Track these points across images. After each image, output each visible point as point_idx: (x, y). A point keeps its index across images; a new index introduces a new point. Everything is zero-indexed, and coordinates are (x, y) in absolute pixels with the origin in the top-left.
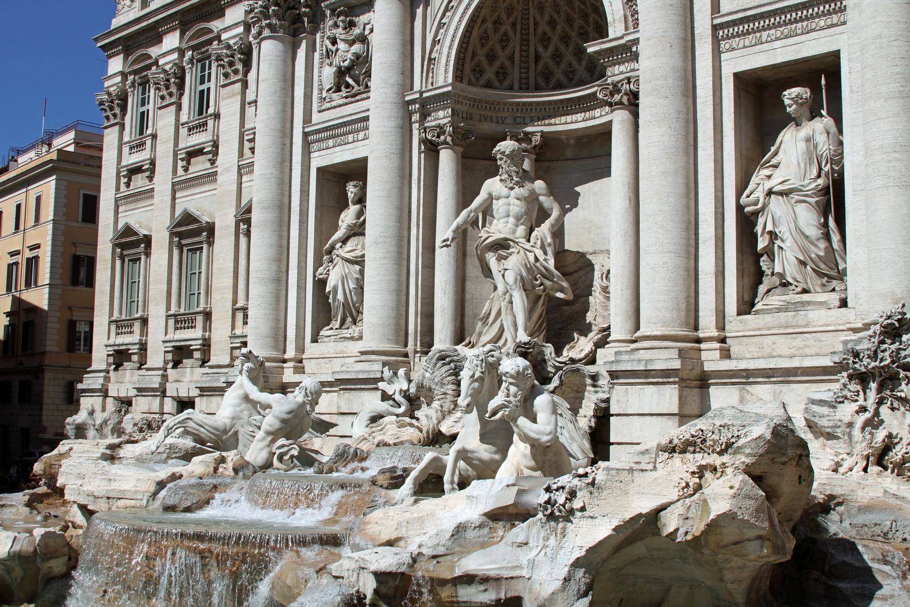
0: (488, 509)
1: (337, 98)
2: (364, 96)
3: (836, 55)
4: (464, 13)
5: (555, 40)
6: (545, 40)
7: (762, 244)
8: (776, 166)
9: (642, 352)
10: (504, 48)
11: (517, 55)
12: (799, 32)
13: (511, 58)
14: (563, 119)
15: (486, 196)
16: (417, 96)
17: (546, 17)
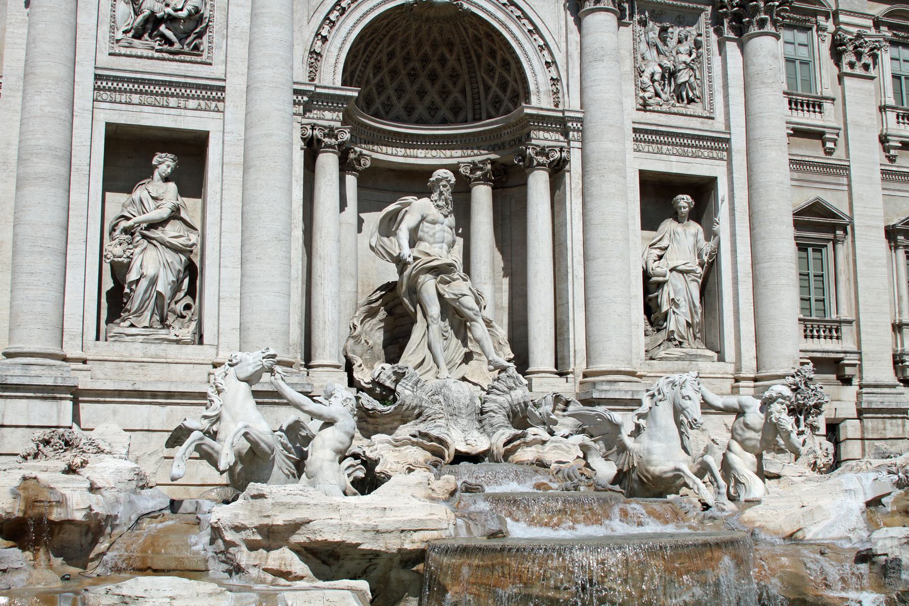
0: (870, 497)
1: (141, 47)
2: (193, 58)
3: (713, 180)
4: (359, 20)
5: (385, 70)
6: (378, 68)
7: (665, 308)
8: (666, 248)
9: (621, 384)
10: (352, 64)
11: (357, 72)
12: (690, 155)
13: (352, 74)
14: (390, 150)
15: (420, 218)
16: (313, 89)
17: (390, 49)
